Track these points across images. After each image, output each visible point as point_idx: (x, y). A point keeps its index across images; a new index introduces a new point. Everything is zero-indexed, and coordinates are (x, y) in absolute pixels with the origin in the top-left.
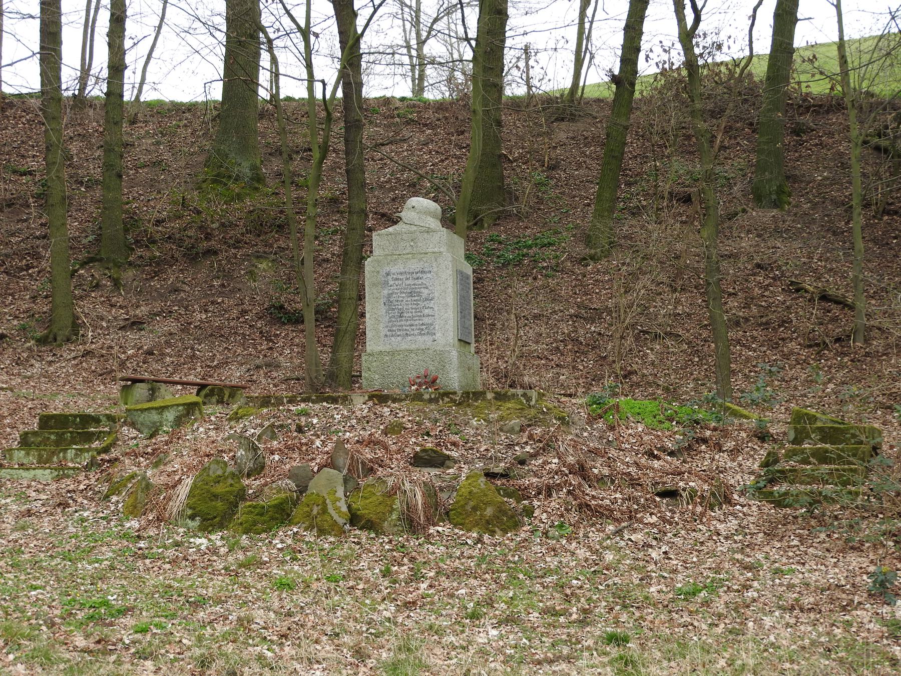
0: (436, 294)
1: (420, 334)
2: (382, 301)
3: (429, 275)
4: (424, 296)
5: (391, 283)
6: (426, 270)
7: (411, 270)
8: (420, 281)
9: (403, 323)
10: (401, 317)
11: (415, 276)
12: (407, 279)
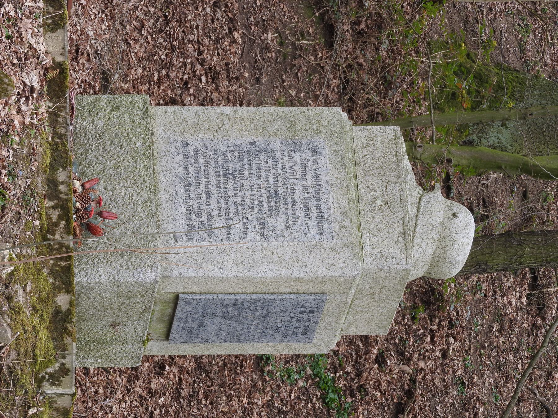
0: (273, 245)
1: (189, 212)
2: (260, 139)
3: (314, 231)
4: (271, 221)
5: (297, 157)
6: (325, 226)
7: (323, 197)
8: (301, 213)
9: (213, 178)
10: (226, 174)
11: (312, 203)
12: (305, 189)
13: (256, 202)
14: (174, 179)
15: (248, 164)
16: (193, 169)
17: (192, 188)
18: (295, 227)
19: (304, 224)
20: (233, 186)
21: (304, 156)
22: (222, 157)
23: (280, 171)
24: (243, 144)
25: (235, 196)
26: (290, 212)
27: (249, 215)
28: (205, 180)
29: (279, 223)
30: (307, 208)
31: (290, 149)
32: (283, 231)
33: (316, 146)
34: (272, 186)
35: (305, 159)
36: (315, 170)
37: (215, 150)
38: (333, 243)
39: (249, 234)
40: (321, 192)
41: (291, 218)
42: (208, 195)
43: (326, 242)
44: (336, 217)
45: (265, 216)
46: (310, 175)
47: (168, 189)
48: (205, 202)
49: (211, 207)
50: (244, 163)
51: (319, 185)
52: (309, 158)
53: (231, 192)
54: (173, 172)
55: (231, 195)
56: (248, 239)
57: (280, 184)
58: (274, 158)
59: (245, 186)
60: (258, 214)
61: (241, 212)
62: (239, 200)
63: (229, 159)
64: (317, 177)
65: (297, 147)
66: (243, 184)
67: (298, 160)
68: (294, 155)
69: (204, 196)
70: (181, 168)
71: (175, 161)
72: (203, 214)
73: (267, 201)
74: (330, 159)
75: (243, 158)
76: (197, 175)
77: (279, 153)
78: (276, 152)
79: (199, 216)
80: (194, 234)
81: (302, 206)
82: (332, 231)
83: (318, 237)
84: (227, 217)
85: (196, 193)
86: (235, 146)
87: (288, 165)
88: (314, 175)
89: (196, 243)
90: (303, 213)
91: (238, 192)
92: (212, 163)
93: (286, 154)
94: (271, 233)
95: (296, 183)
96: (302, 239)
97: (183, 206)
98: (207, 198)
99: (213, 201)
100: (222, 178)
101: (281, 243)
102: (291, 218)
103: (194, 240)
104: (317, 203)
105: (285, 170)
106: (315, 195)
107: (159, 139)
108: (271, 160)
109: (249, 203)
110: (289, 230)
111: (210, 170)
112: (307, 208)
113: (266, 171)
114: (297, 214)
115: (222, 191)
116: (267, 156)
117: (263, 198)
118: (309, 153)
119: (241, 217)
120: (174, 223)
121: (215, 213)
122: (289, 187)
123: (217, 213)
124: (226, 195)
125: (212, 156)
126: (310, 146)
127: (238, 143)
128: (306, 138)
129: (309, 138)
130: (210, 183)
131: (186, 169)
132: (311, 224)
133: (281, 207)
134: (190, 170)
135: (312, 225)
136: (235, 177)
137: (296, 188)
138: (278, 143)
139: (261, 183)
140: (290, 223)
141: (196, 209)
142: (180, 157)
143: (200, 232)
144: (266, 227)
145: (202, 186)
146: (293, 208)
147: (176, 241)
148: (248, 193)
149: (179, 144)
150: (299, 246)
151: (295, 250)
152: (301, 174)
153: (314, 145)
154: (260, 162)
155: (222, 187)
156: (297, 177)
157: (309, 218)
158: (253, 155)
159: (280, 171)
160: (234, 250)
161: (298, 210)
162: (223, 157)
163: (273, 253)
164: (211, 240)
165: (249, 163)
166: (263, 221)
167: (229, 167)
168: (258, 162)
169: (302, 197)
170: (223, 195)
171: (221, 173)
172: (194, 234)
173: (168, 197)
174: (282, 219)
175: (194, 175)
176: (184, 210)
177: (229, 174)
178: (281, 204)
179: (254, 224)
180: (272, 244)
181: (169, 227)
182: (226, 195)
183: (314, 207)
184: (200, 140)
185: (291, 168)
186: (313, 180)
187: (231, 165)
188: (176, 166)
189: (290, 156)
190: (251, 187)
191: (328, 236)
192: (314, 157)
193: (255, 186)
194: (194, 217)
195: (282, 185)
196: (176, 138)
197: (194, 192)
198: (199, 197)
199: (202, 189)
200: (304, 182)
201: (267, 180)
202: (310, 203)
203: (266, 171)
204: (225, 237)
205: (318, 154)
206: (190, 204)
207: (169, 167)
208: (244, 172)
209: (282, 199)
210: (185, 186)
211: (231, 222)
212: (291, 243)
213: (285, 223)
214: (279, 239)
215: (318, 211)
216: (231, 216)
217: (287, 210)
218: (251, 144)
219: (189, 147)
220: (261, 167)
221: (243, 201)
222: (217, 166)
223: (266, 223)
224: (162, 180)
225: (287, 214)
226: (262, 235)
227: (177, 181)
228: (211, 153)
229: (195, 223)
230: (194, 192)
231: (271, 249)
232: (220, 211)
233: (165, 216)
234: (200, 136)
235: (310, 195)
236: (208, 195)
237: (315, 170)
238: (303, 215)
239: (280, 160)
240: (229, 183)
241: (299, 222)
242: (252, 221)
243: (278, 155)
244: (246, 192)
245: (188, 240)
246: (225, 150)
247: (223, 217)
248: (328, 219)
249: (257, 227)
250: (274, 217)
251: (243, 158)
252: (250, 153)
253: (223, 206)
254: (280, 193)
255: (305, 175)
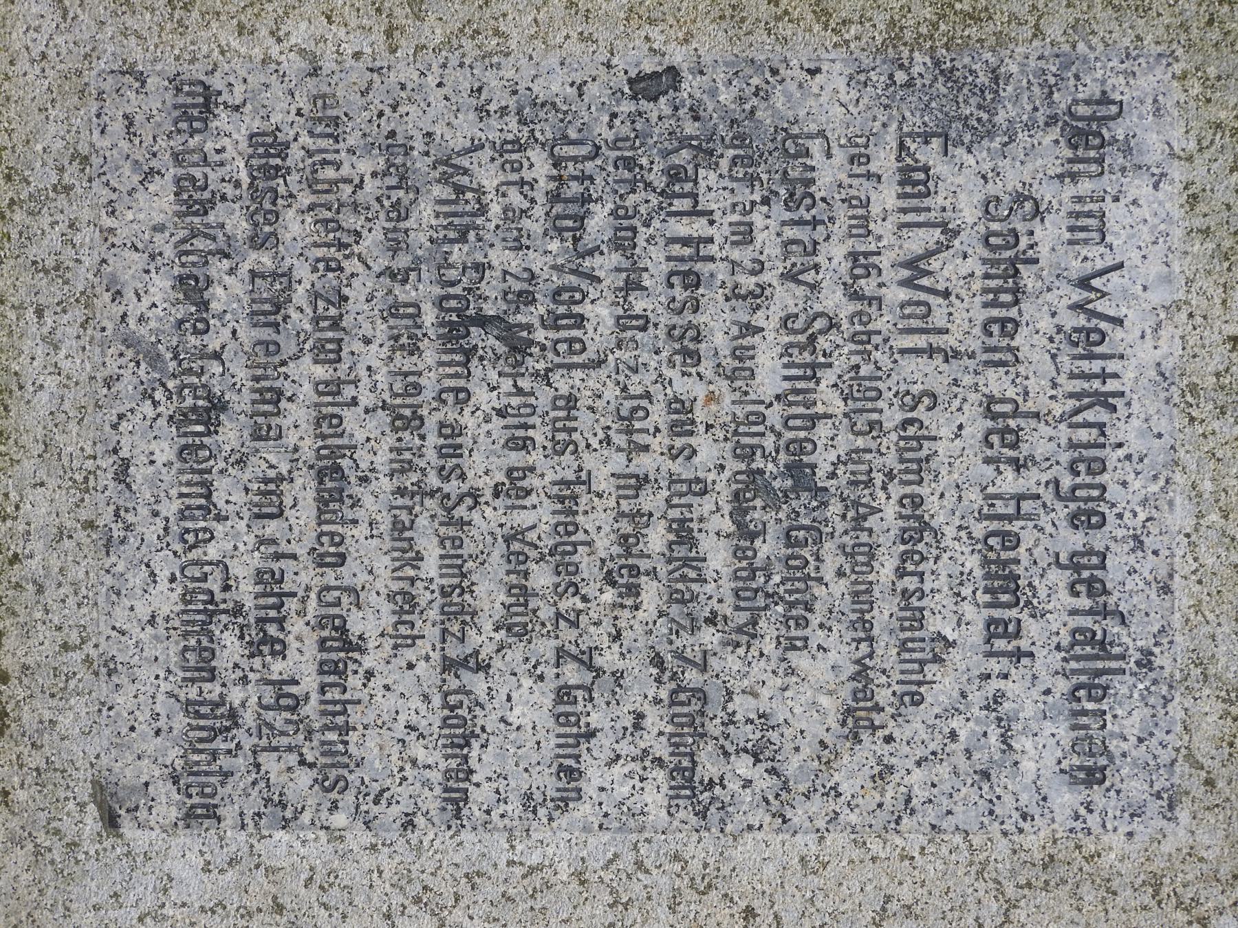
0: (759, 857)
1: (204, 611)
2: (704, 52)
3: (1043, 750)
4: (751, 680)
5: (962, 183)
6: (1127, 715)
7: (1126, 489)
8: (958, 619)
9: (371, 358)
10: (458, 327)
11: (1048, 538)
12: (1004, 431)
13: (657, 539)
14: (112, 367)
15: (617, 244)
16: (237, 286)
17: (230, 434)
18: (916, 724)
19: (977, 698)
20: (502, 413)
21: (1013, 177)
22: (439, 191)
23: (833, 299)
24: (592, 89)
25: (514, 488)
26: (884, 612)
27: (599, 636)
28: (320, 372)
29: (803, 693)
30: (1004, 583)
31: (914, 122)
32: (826, 755)
33: (1105, 100)
34: (774, 416)
35: (1020, 199)
36: (1084, 283)
37: (393, 145)
38: (1167, 847)
39: (594, 776)
40: (1112, 456)
41: (887, 653)
42: (333, 478)
43: (1116, 840)
44: (1207, 648)
45: (709, 637)
46: (1046, 324)
47: (72, 441)
48: (309, 540)
49: (352, 574)
50: (588, 241)
51: (1104, 401)
52: (1046, 192)
53: (485, 465)
54: (106, 310)
55: (486, 484)
56: (584, 811)
57: (828, 398)
58: (799, 192)
59: (584, 419)
60: (662, 627)
61: (546, 613)
62: (539, 517)
63: (483, 210)
64: (1089, 339)
65: (959, 105)
66: (571, 401)
67: (969, 212)
68: (940, 167)
69: (302, 492)
70: (161, 286)
71: (123, 233)
72: (296, 626)
73: (727, 525)
74: (1193, 200)
75: (585, 199)
76: (266, 334)
77: (840, 156)
78: (816, 146)
79: (267, 644)
80: (226, 775)
81: (973, 563)
82: (1165, 756)
83: (1066, 799)
84: (454, 651)
85: (256, 467)
86: (531, 108)
87: (894, 245)
88: (1072, 321)
89: (238, 840)
90: (976, 617)
91: (536, 457)
92: (372, 240)
93: (884, 160)
94: (743, 766)
95: (939, 385)
96: (959, 818)
97: (165, 566)
98: (323, 504)
99: (362, 530)
100: (430, 356)
101: (806, 842)
102: (887, 653)
103: (229, 813)
104: (1075, 540)
105: (868, 286)
106: (1067, 482)
107: (23, 64)
108: (778, 209)
109: (605, 544)
110: (871, 746)
111: (356, 294)
112: (1004, 583)
113: (735, 294)
114: (934, 624)
115: (431, 455)
116: (751, 180)
117: (707, 504)
118: (1050, 151)
119: (545, 647)
120: (103, 689)
121: (369, 622)
122: (892, 417)
123: (388, 620)
124: (453, 487)
125: (370, 186)
126: (1062, 100)
127: (556, 86)
128: (1038, 32)
129: (1054, 30)
130: (348, 392)
131: (192, 288)
132: (1021, 696)
133: (828, 573)
134: (219, 298)
135: (1029, 710)
136: (518, 347)
137: (939, 423)
138: (835, 78)
139: (700, 391)
140: (883, 696)
141: (246, 592)
142: (158, 202)
143: (269, 762)
144: (714, 728)
145: (297, 417)
146: (910, 583)
147: (111, 821)
148: (604, 468)
149: (155, 101)
150: (931, 869)
151: (906, 894)
152: (981, 315)
153: (1091, 89)
154: (699, 227)
155: (431, 423)
156: (948, 341)
157: (1018, 655)
158: (660, 182)
159: (833, 299)
160: (490, 890)
161: (944, 599)
162: (446, 193)
163: (749, 913)
164: (340, 819)
165: (623, 241)
166: (692, 677)
167: (480, 268)
168: (682, 228)
169: (974, 497)
170: (433, 481)
171: (429, 316)
172: (226, 775)
173: (64, 500)
174: (827, 663)
175: (248, 335)
176: (166, 600)
177: (482, 321)
178: (829, 546)
179: (632, 700)
180: (747, 850)
181: (65, 721)
182: (453, 487)
183: (1054, 575)
184: (294, 65)
185: (915, 267)
186: (1064, 359)
187: (499, 257)
188: (128, 266)
189: (915, 181)
190: (627, 422)
191: (1136, 789)
192: (1085, 187)
193: (658, 415)
194: (230, 648)
195: (838, 406)
196: (137, 54)
197: (241, 462)
198: (269, 502)
199: (291, 438)
200: (996, 382)
201: (740, 368)
202: (1028, 538)
203: (735, 294)
204: (431, 801)
205: (1114, 158)
206: (213, 552)
207: (82, 277)
208: (586, 309)
209: (835, 508)
210: (180, 420)
211: (478, 684)
212: (875, 846)
213: (846, 692)
214: (797, 816)
215: (1085, 602)
216: (483, 638)
217: (862, 597)
218: (647, 86)
219: (223, 120)
220: (704, 268)
221: (567, 527)
222: (403, 261)
223: (716, 695)
224: (31, 372)
225: (863, 629)
226: (687, 784)
227: (127, 386)
228: (364, 167)
229: (236, 696)
230: (241, 462)
231: (740, 887)
232: (405, 603)
233: (43, 646)
234: (299, 33)
235: (1032, 480)
236: (333, 478)
237: (1084, 283)
238: (976, 634)
239: (841, 211)
240: (482, 397)
241: (943, 686)
242: (618, 676)
243: (829, 173)
244: (589, 461)
245: (190, 817)
246: (460, 143)
247: (423, 646)
248: (1147, 661)
249: (655, 720)
250: (769, 647)
251: (585, 199)
252: (630, 163)
253: (431, 567)
254: (823, 460)
255: (1009, 326)
